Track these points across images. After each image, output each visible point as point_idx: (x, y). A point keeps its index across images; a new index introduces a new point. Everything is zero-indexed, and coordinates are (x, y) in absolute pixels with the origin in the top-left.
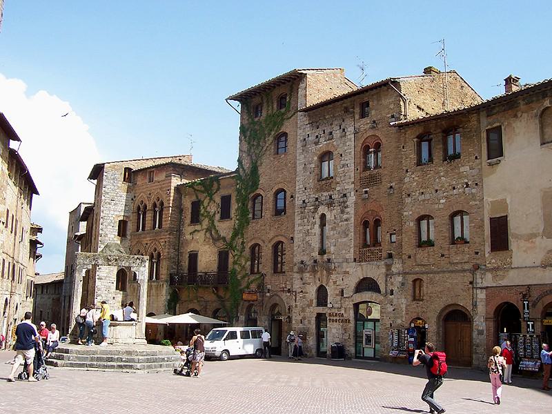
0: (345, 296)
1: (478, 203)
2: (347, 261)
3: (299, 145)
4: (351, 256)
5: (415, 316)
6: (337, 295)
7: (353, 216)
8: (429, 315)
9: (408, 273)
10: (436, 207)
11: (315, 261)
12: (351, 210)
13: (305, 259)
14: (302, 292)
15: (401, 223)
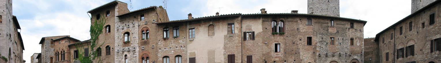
1: (185, 53)
3: (116, 30)
10: (170, 53)
12: (137, 54)
15: (157, 59)
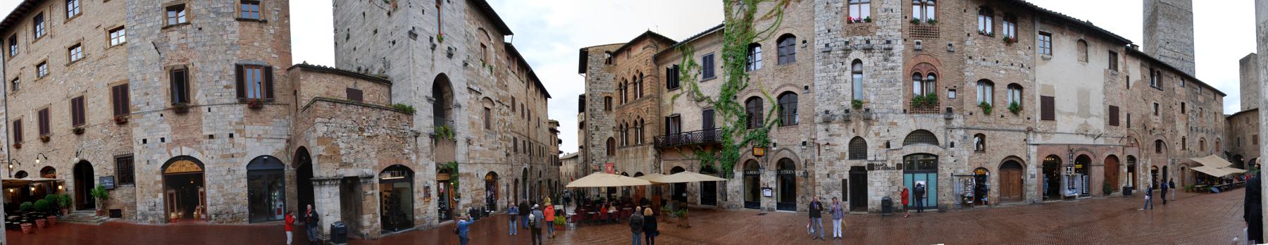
0: (891, 148)
2: (894, 112)
4: (900, 106)
5: (977, 166)
6: (880, 147)
7: (901, 65)
8: (991, 165)
9: (968, 129)
11: (847, 111)
12: (898, 60)
13: (832, 108)
14: (828, 144)
